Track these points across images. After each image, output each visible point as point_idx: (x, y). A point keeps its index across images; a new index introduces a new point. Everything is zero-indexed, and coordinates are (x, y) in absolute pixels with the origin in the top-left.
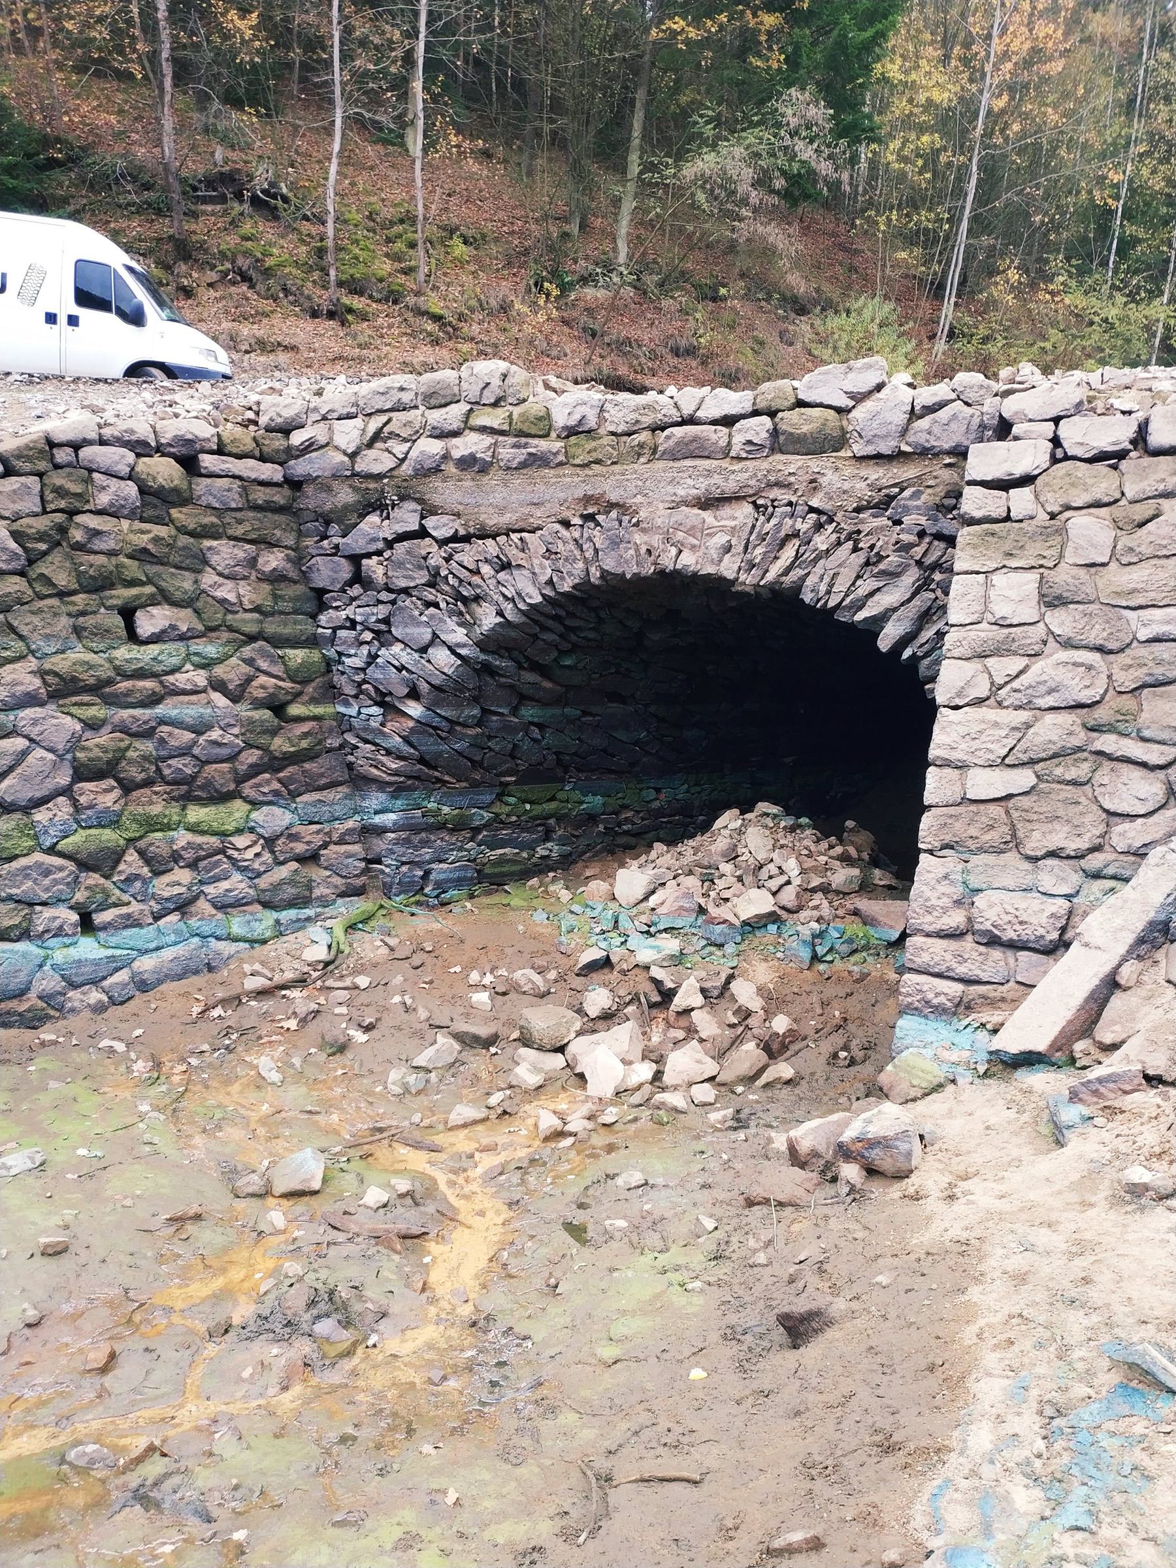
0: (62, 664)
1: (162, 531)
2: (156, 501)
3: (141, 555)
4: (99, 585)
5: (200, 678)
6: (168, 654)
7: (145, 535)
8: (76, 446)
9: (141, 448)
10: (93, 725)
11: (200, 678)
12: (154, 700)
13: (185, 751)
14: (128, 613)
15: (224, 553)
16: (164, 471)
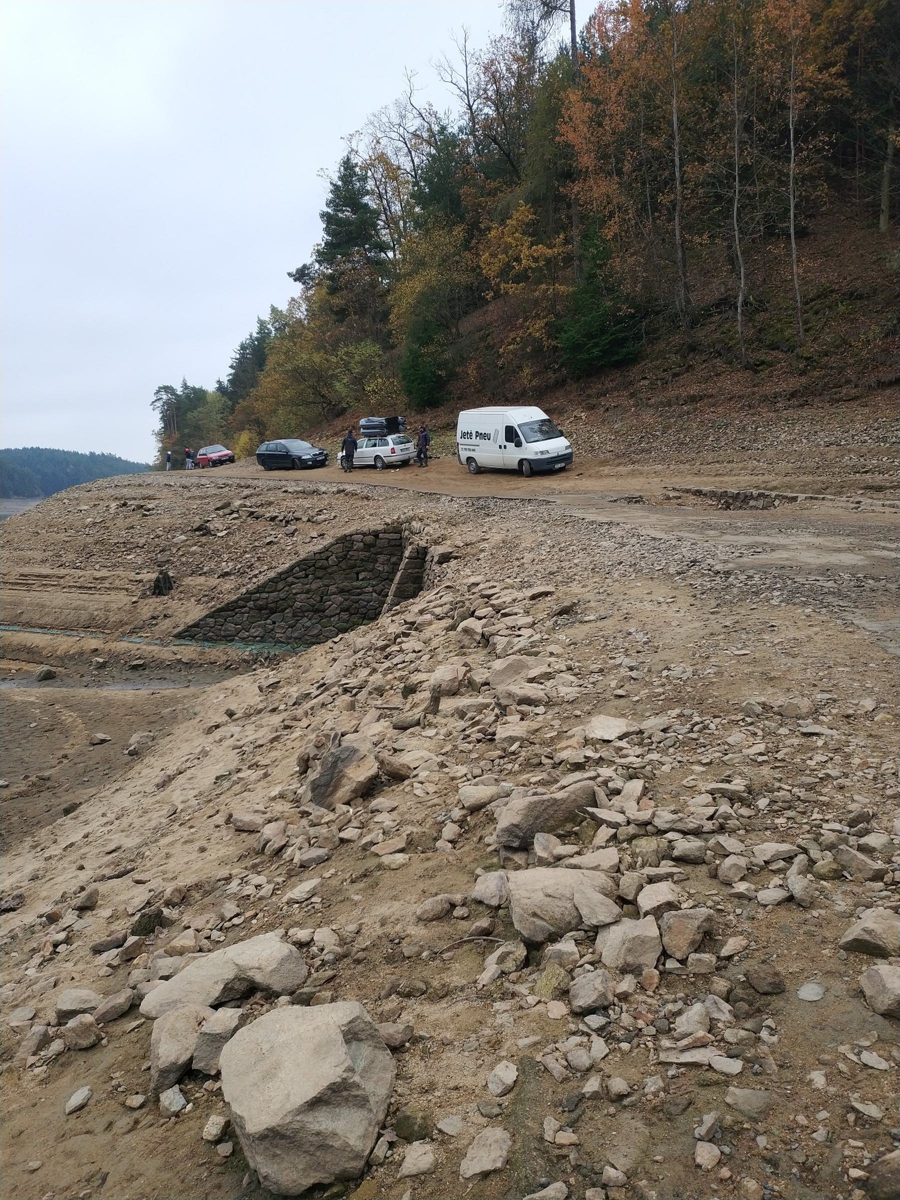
0: (341, 586)
1: (367, 554)
2: (368, 547)
3: (362, 560)
4: (353, 567)
5: (371, 589)
6: (364, 583)
7: (362, 555)
8: (351, 535)
9: (364, 534)
10: (346, 600)
11: (371, 589)
12: (359, 594)
13: (365, 607)
14: (357, 574)
15: (382, 558)
16: (369, 539)
